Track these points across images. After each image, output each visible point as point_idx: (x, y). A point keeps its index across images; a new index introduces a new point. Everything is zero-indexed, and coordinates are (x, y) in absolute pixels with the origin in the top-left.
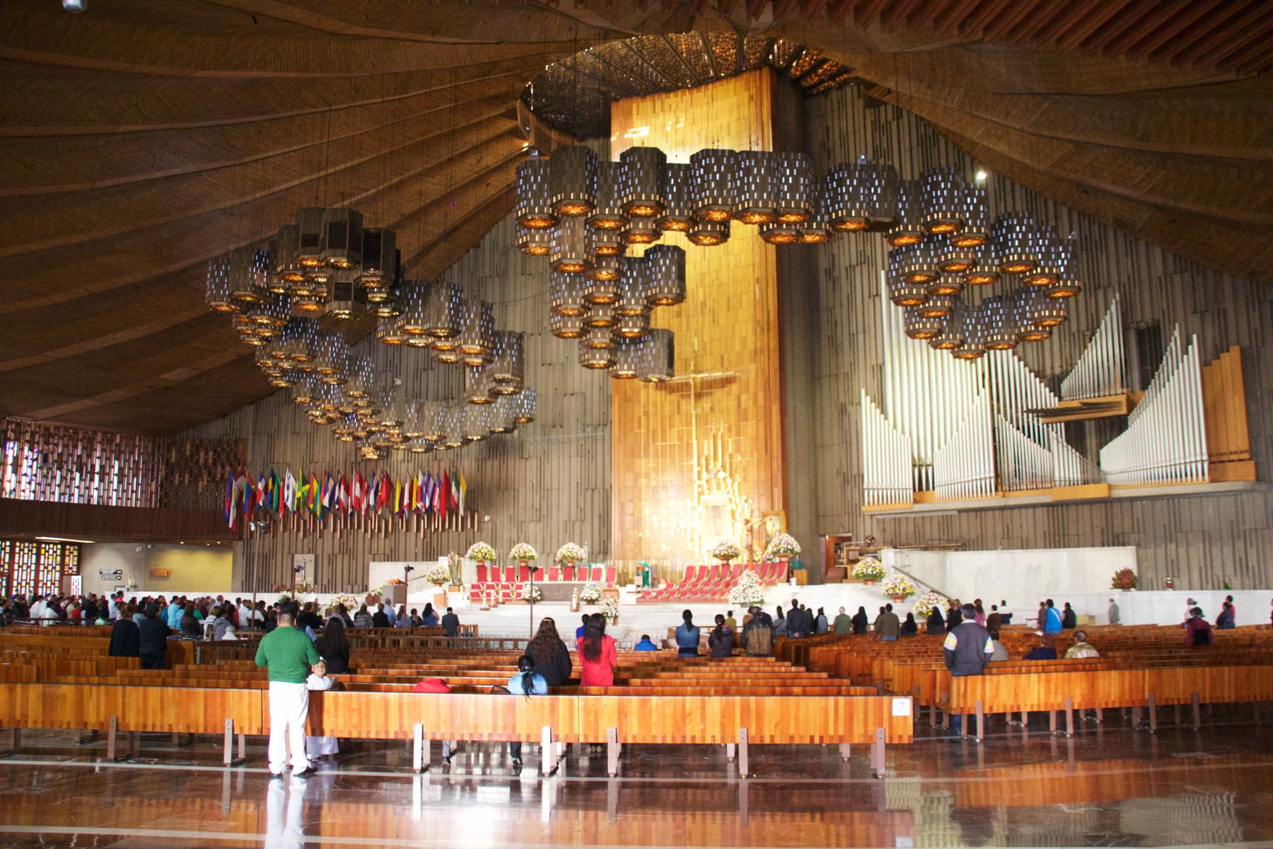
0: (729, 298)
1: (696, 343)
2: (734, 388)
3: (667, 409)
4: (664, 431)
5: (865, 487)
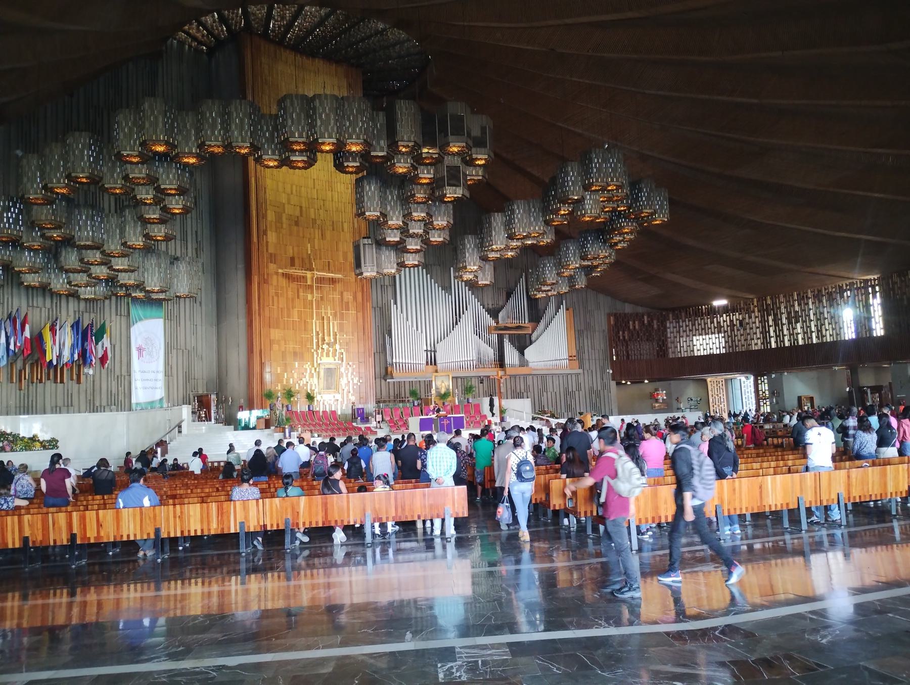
0: (333, 222)
1: (309, 249)
2: (339, 287)
3: (290, 293)
4: (288, 309)
5: (394, 361)
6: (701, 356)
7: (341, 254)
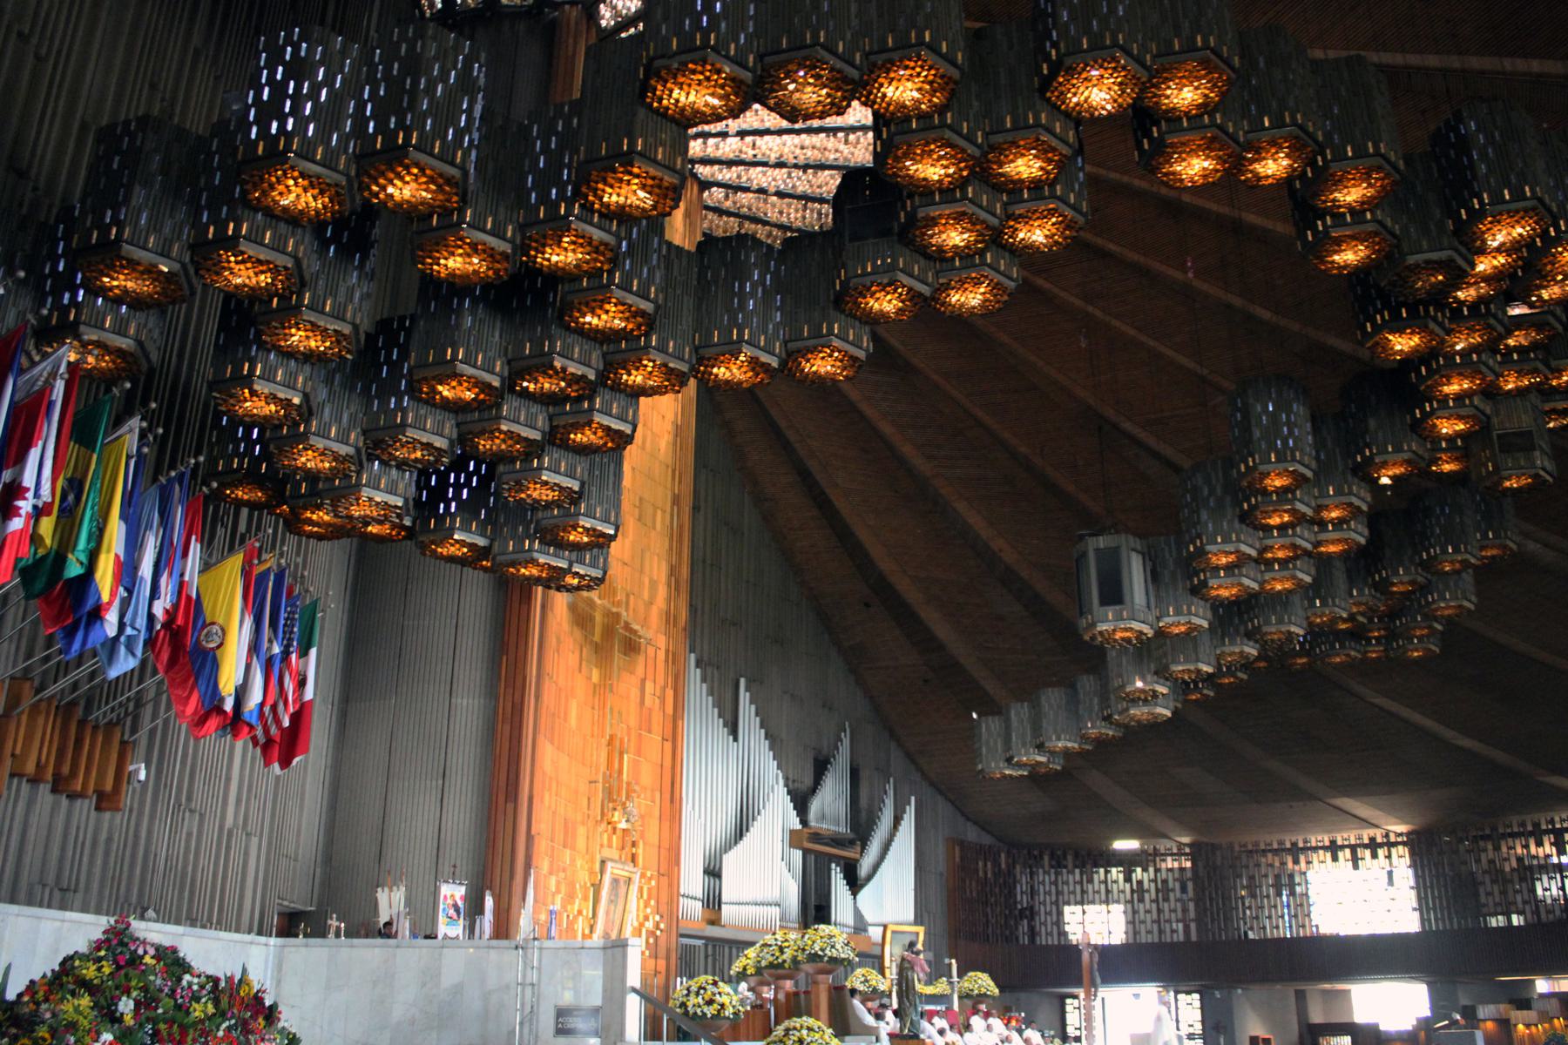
6: (1305, 938)
7: (646, 581)
